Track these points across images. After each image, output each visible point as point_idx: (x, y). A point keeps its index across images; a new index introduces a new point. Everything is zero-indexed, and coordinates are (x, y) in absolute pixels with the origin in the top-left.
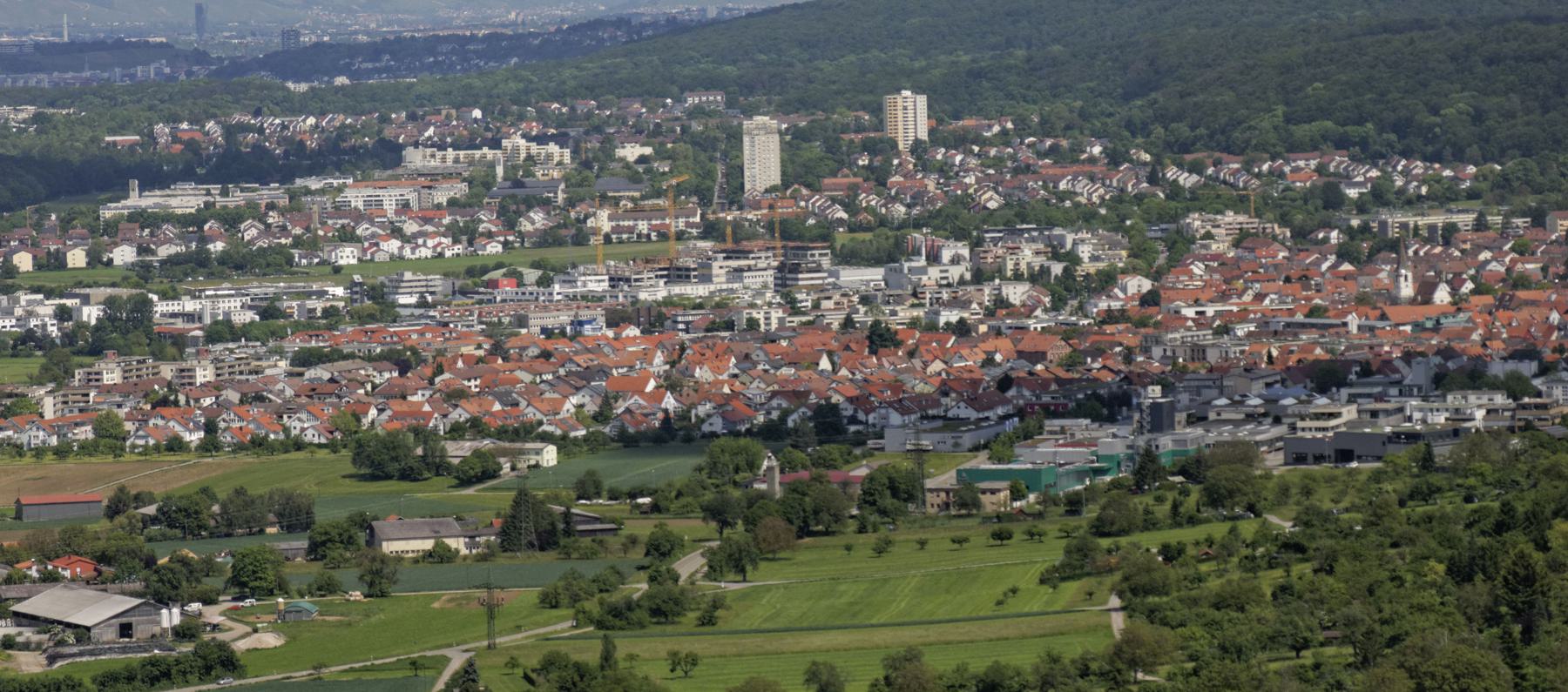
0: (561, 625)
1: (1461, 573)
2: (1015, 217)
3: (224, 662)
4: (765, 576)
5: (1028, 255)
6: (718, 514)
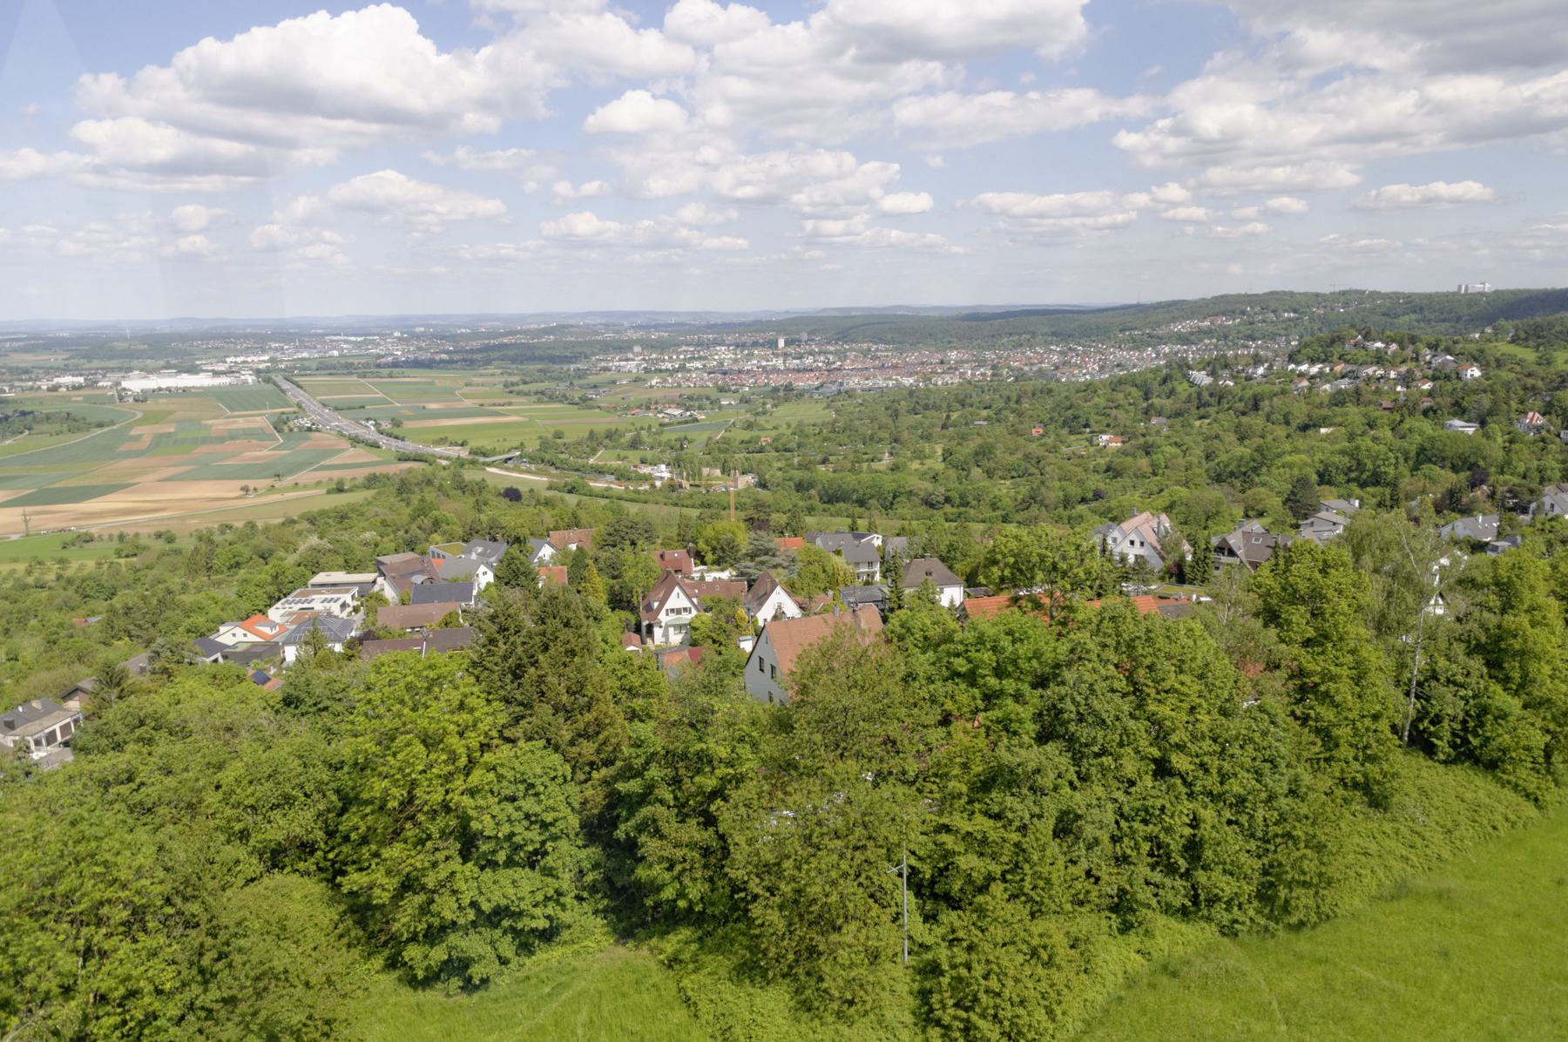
0: (748, 415)
1: (887, 409)
2: (820, 353)
3: (696, 420)
4: (780, 408)
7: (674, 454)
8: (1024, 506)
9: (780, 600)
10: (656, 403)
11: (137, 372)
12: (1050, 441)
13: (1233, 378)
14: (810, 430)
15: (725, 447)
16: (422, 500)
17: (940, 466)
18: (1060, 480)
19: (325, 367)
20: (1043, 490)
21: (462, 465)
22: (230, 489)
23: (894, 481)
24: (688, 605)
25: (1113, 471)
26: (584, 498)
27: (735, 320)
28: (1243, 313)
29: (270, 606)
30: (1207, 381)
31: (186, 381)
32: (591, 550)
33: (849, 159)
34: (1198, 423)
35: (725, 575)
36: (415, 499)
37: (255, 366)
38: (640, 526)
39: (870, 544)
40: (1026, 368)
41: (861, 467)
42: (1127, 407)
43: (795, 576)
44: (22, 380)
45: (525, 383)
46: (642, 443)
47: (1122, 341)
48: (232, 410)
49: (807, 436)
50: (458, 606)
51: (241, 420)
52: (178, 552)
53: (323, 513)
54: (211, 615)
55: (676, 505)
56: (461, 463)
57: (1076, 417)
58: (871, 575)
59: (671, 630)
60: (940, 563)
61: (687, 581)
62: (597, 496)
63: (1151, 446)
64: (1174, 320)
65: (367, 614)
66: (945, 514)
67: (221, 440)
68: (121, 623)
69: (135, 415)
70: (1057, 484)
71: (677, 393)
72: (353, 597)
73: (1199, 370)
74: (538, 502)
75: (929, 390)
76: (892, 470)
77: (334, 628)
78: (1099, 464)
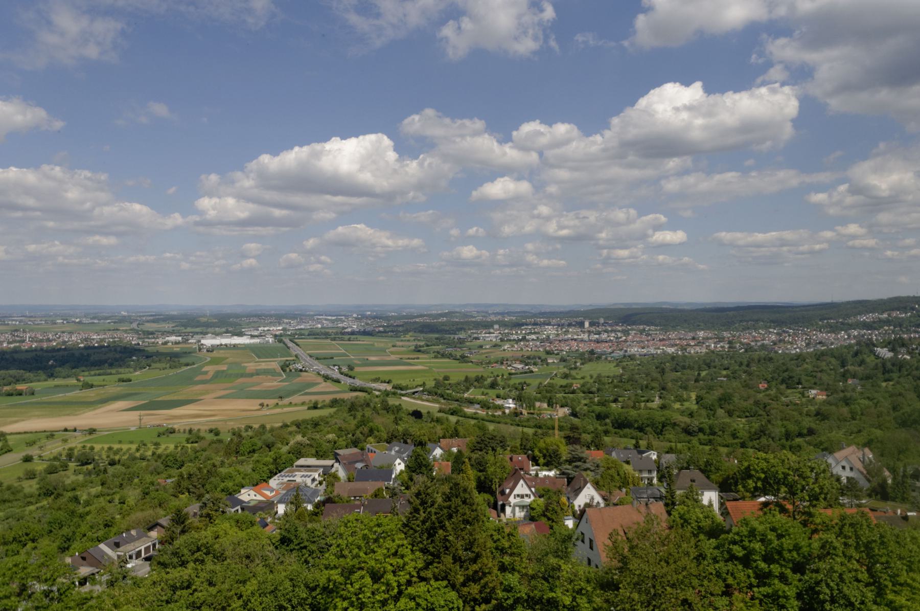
1: (657, 368)
2: (612, 331)
3: (532, 372)
4: (586, 365)
5: (613, 335)
6: (581, 359)
7: (518, 393)
8: (756, 437)
9: (588, 494)
10: (507, 360)
11: (210, 335)
12: (773, 392)
13: (909, 353)
14: (606, 380)
15: (550, 388)
16: (363, 416)
17: (694, 407)
18: (781, 420)
19: (313, 334)
20: (770, 426)
21: (387, 395)
22: (253, 404)
23: (663, 416)
24: (528, 492)
25: (820, 415)
26: (461, 419)
27: (558, 310)
28: (913, 309)
29: (270, 478)
30: (890, 355)
31: (236, 340)
32: (466, 453)
33: (633, 212)
34: (884, 384)
35: (552, 474)
36: (359, 415)
37: (274, 333)
38: (497, 438)
39: (648, 458)
40: (753, 344)
41: (640, 405)
42: (829, 371)
43: (598, 477)
44: (149, 338)
45: (428, 346)
46: (498, 385)
47: (823, 327)
48: (259, 357)
49: (604, 384)
50: (383, 484)
51: (263, 364)
52: (220, 441)
53: (305, 421)
54: (236, 482)
55: (518, 425)
56: (387, 394)
57: (791, 377)
58: (650, 480)
59: (517, 509)
60: (700, 473)
61: (527, 476)
62: (468, 417)
63: (850, 399)
64: (860, 313)
65: (327, 486)
66: (699, 439)
67: (251, 375)
68: (185, 484)
69: (206, 359)
70: (780, 423)
71: (519, 354)
72: (319, 475)
73: (882, 348)
74: (432, 420)
75: (685, 356)
76: (661, 408)
77: (308, 494)
78: (810, 410)
